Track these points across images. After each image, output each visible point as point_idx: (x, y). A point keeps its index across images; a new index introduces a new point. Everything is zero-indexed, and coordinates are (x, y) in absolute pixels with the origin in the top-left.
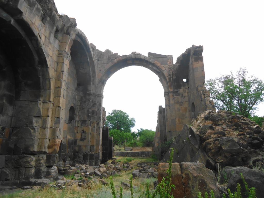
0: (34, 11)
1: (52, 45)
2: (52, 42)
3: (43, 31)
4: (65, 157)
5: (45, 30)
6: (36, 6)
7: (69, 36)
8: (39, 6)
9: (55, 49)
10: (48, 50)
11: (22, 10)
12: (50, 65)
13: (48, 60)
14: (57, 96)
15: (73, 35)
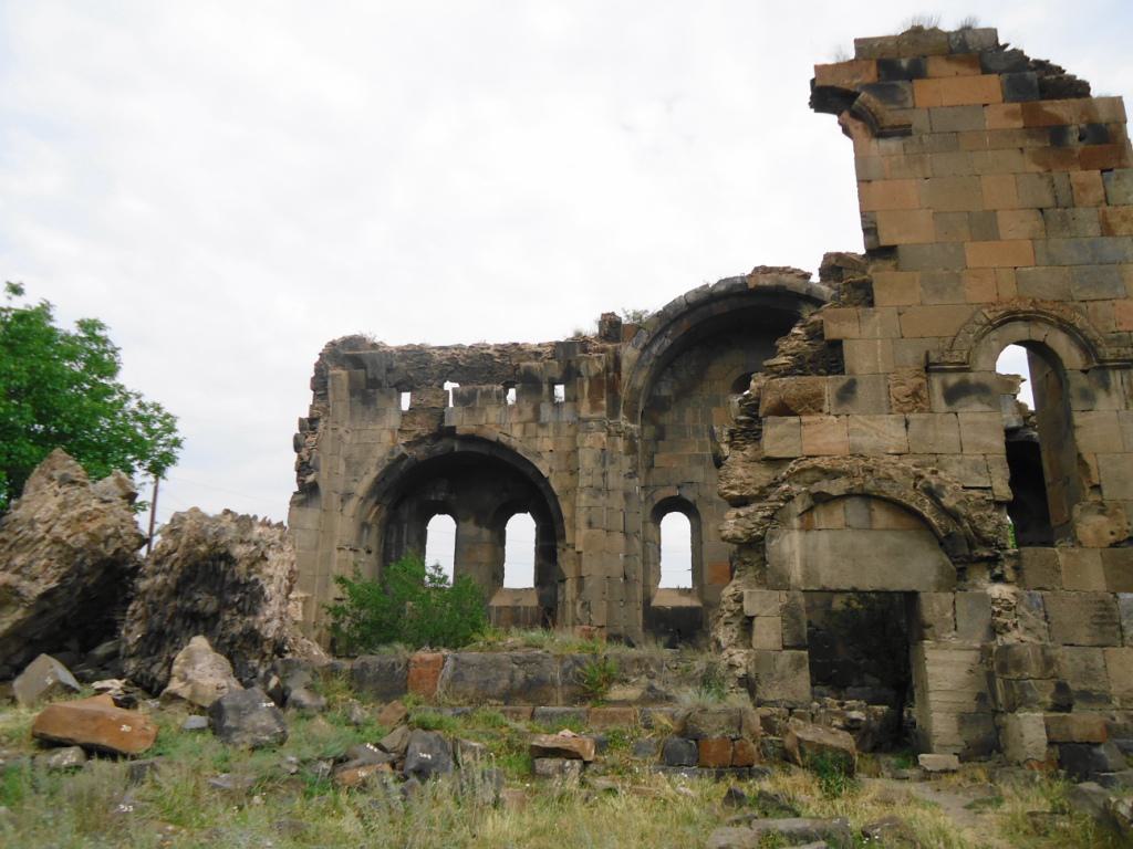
0: (478, 405)
1: (551, 426)
2: (547, 420)
3: (514, 418)
4: (834, 671)
5: (520, 412)
6: (479, 393)
7: (578, 379)
8: (484, 388)
9: (564, 427)
10: (539, 445)
11: (453, 425)
12: (551, 470)
13: (539, 465)
14: (574, 527)
15: (590, 367)
